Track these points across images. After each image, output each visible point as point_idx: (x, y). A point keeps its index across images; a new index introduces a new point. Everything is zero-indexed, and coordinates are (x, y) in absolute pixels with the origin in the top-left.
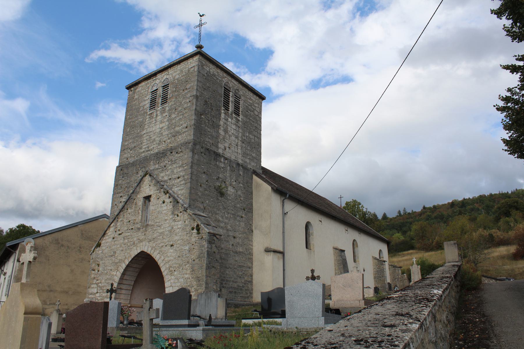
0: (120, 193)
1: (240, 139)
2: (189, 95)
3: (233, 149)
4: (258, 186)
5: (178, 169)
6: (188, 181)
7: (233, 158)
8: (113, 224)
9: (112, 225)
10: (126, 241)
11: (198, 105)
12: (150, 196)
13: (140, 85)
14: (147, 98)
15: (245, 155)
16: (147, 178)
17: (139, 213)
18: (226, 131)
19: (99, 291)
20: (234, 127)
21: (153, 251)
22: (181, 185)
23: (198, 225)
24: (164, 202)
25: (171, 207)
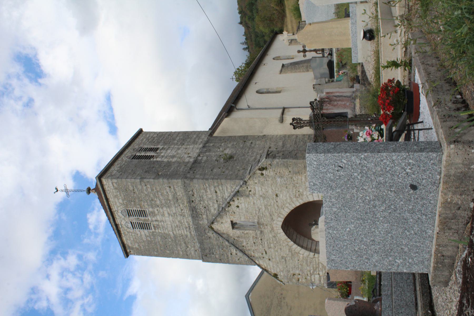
0: (228, 256)
1: (180, 146)
2: (140, 187)
3: (189, 151)
4: (223, 131)
5: (208, 194)
6: (219, 182)
7: (198, 151)
8: (256, 261)
9: (258, 263)
12: (232, 222)
14: (139, 233)
15: (195, 143)
16: (215, 226)
17: (247, 233)
18: (173, 157)
19: (318, 273)
20: (169, 151)
21: (281, 216)
22: (222, 190)
23: (260, 169)
24: (238, 207)
25: (242, 198)
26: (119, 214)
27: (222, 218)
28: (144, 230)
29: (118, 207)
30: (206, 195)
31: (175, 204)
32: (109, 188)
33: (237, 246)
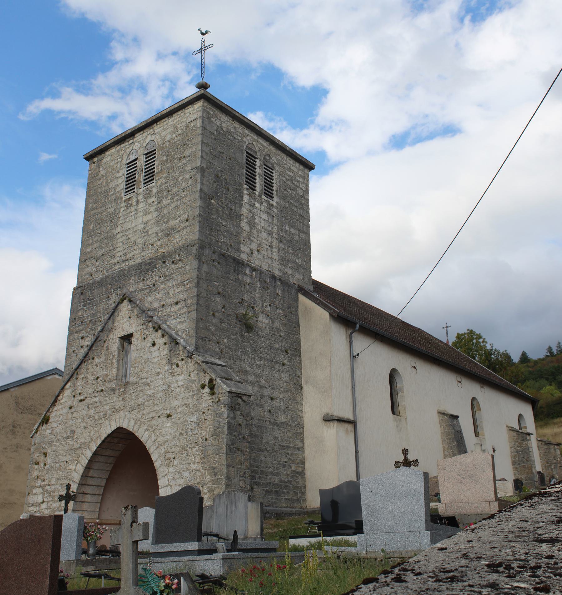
0: (80, 331)
1: (276, 236)
2: (189, 167)
3: (264, 252)
5: (175, 288)
6: (192, 308)
7: (265, 267)
8: (69, 384)
9: (67, 386)
10: (92, 411)
11: (205, 182)
12: (131, 335)
13: (108, 153)
14: (121, 174)
15: (284, 261)
16: (125, 306)
18: (252, 224)
19: (45, 500)
20: (265, 216)
22: (181, 314)
23: (211, 381)
24: (154, 344)
25: (166, 351)
26: (149, 136)
27: (138, 317)
28: (125, 183)
29: (160, 134)
31: (162, 231)
32: (188, 115)
33: (94, 348)
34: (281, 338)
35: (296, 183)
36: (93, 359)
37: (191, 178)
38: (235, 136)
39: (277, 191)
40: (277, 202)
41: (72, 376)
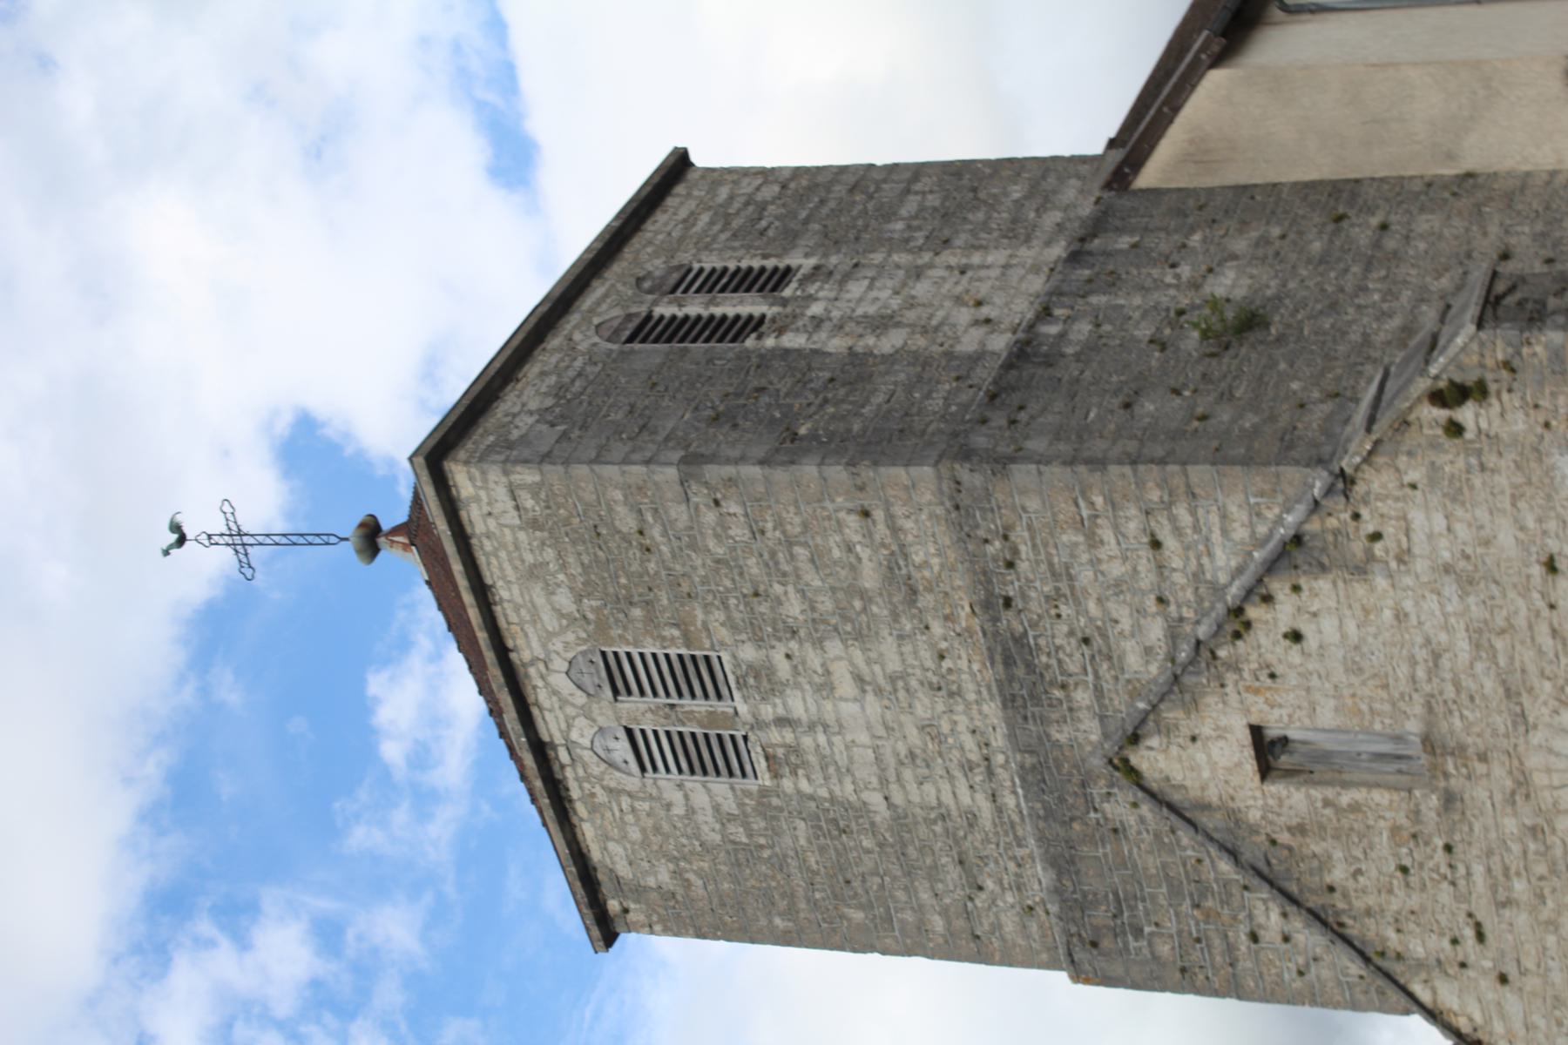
0: (1230, 948)
1: (927, 257)
3: (983, 289)
4: (1199, 154)
5: (1102, 553)
6: (1178, 481)
7: (1037, 284)
10: (1520, 887)
11: (735, 453)
12: (1256, 731)
13: (596, 855)
14: (677, 797)
15: (1017, 232)
16: (1152, 759)
17: (1355, 808)
18: (882, 323)
20: (856, 289)
22: (1196, 528)
23: (1437, 398)
24: (1296, 636)
25: (1323, 584)
26: (553, 679)
27: (1193, 705)
28: (712, 778)
30: (1095, 562)
31: (895, 617)
32: (492, 523)
33: (1293, 888)
34: (1292, 236)
35: (736, 205)
36: (1331, 889)
37: (717, 503)
38: (571, 373)
39: (765, 257)
40: (807, 255)
41: (1388, 976)
